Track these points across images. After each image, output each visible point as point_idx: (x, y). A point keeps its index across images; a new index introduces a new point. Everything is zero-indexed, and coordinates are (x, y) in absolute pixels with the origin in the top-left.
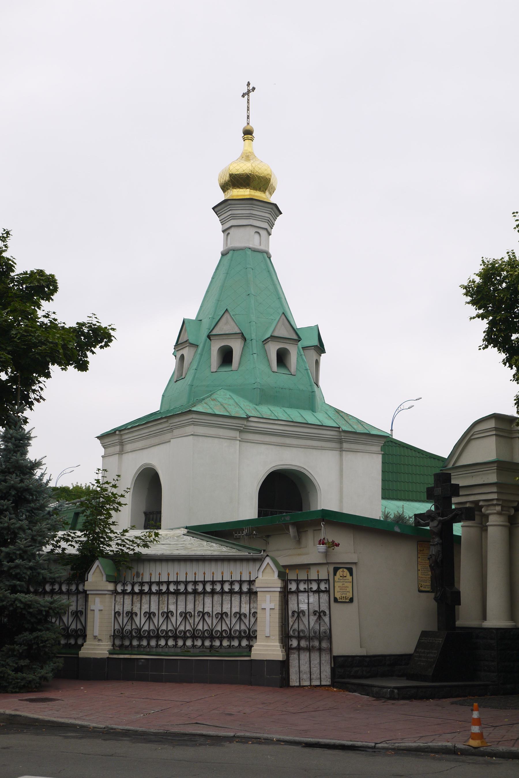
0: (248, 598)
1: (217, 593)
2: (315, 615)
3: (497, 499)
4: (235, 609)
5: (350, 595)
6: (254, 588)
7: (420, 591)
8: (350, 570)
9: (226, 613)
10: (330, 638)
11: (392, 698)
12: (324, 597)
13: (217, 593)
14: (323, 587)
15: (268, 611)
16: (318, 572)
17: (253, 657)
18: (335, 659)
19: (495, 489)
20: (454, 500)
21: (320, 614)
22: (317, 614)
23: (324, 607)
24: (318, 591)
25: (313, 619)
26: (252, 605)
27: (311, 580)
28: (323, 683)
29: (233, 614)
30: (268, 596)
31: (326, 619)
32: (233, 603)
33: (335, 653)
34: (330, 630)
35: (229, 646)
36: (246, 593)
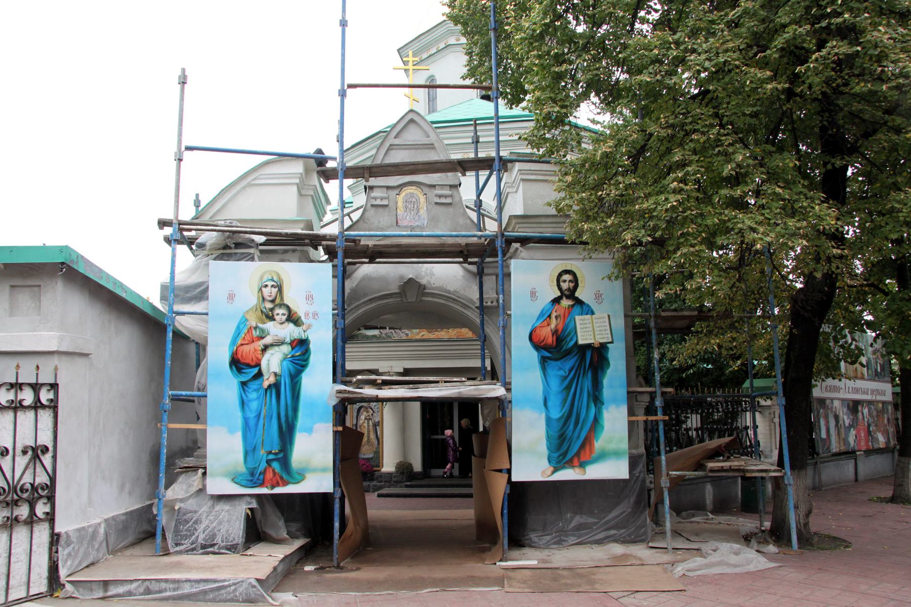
2: (24, 452)
10: (51, 499)
21: (36, 452)
22: (30, 453)
25: (22, 461)
27: (22, 384)
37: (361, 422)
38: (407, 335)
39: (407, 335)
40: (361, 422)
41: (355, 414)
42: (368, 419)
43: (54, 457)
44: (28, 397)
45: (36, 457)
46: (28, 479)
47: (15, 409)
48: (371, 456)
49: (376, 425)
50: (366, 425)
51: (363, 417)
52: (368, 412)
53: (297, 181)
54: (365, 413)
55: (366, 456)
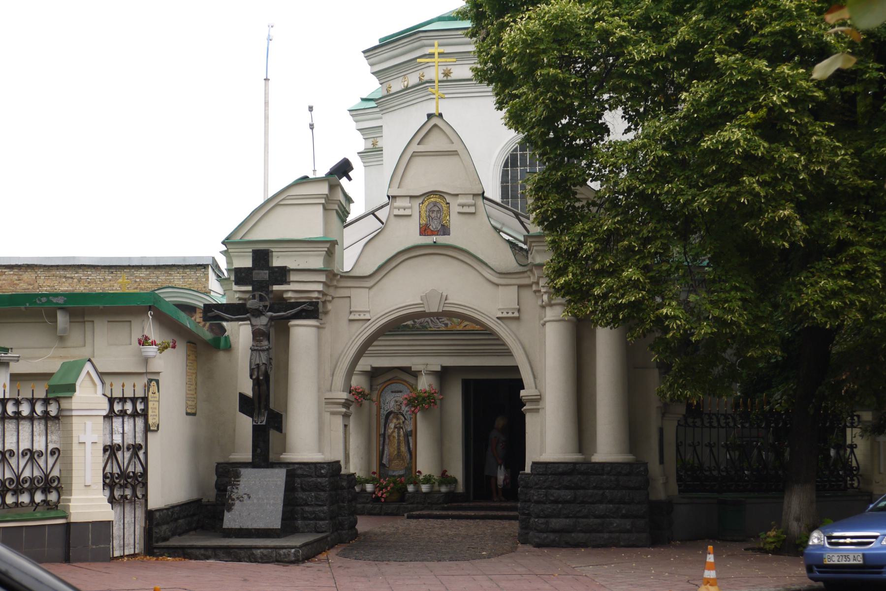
0: (42, 427)
1: (24, 418)
2: (128, 449)
3: (319, 292)
4: (25, 445)
5: (156, 421)
6: (53, 410)
7: (188, 414)
8: (157, 382)
9: (11, 452)
10: (145, 485)
11: (296, 561)
12: (140, 422)
13: (24, 418)
14: (140, 407)
15: (89, 446)
16: (123, 386)
17: (73, 519)
18: (150, 515)
19: (323, 278)
20: (276, 288)
21: (135, 449)
23: (139, 440)
24: (135, 415)
25: (127, 455)
26: (49, 437)
28: (137, 552)
29: (20, 452)
30: (89, 423)
31: (141, 454)
32: (21, 432)
33: (153, 504)
34: (145, 469)
35: (16, 504)
36: (40, 418)
37: (390, 431)
38: (446, 325)
39: (446, 325)
40: (390, 431)
41: (383, 421)
42: (398, 428)
43: (146, 453)
44: (129, 407)
45: (135, 454)
46: (131, 469)
47: (123, 417)
48: (402, 472)
49: (408, 435)
50: (395, 435)
51: (392, 426)
52: (398, 419)
53: (323, 201)
54: (395, 421)
55: (396, 473)
